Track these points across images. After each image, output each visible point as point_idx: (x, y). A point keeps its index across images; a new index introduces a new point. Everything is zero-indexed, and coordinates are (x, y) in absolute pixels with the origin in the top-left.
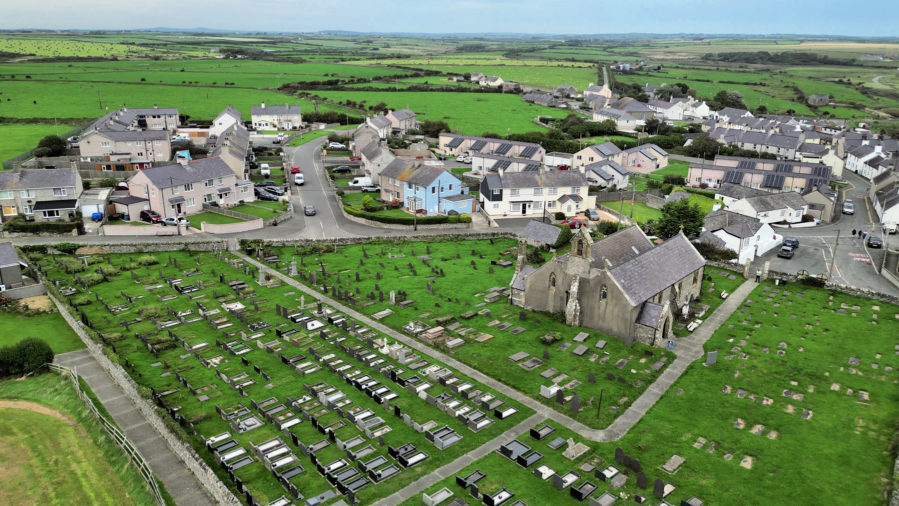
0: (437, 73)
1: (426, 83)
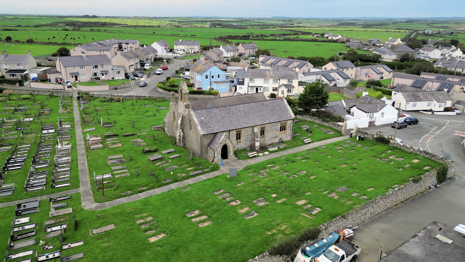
0: (309, 33)
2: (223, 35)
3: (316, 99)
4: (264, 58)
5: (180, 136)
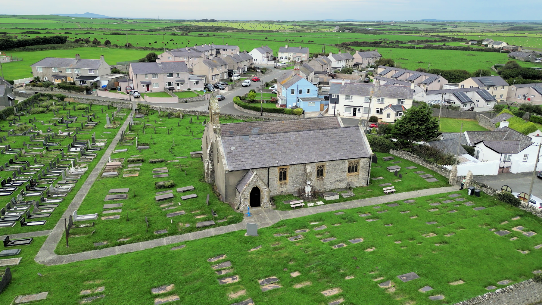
0: (462, 40)
2: (347, 41)
3: (417, 130)
4: (384, 69)
5: (208, 169)
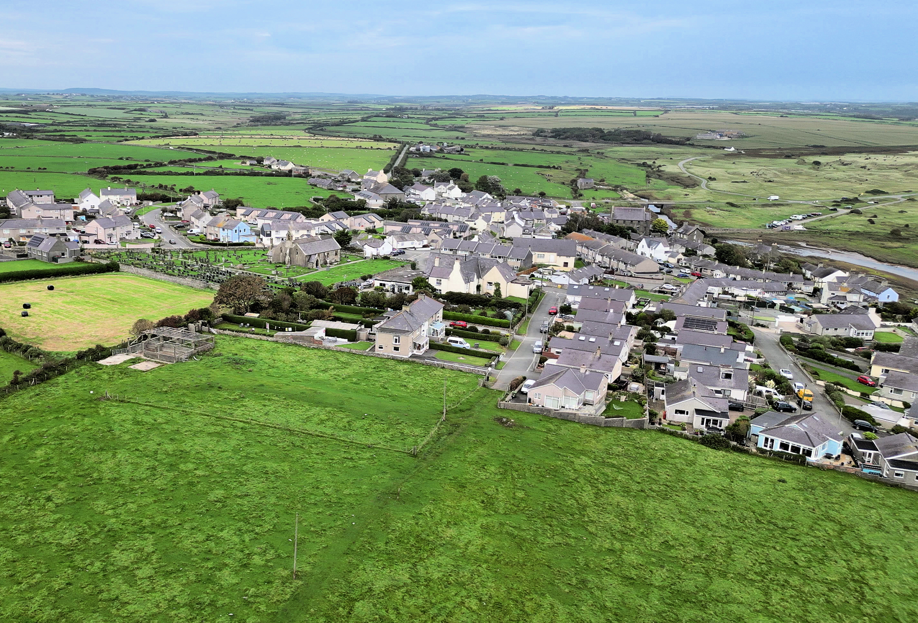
0: (230, 156)
1: (221, 167)
